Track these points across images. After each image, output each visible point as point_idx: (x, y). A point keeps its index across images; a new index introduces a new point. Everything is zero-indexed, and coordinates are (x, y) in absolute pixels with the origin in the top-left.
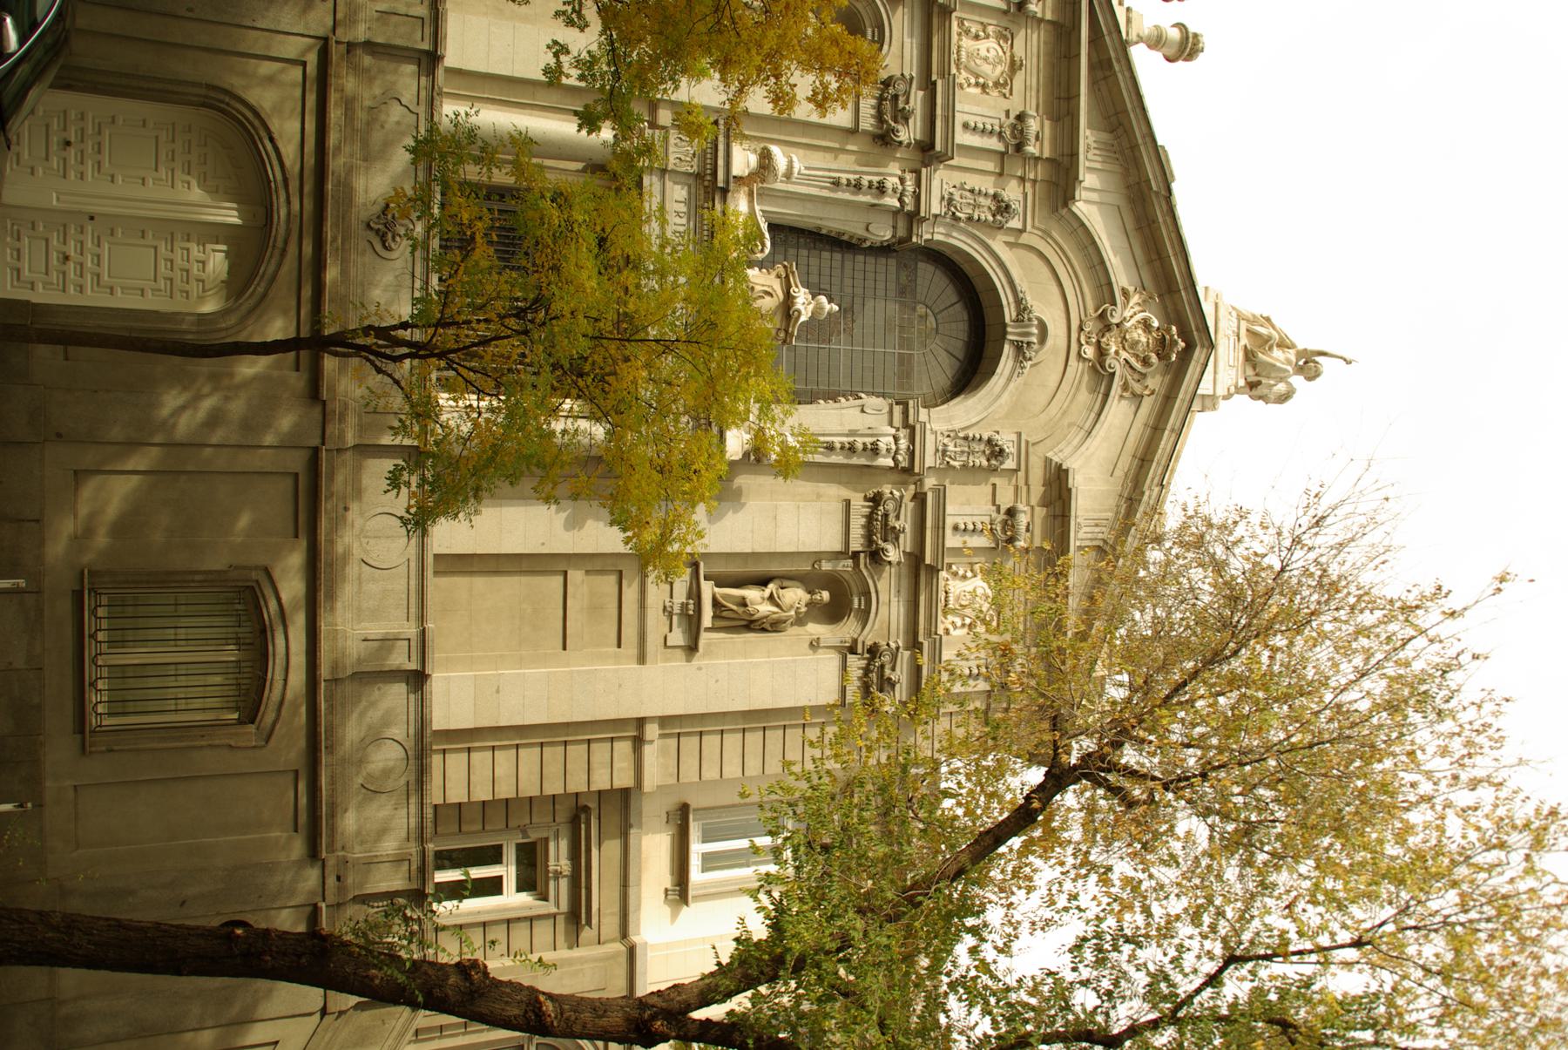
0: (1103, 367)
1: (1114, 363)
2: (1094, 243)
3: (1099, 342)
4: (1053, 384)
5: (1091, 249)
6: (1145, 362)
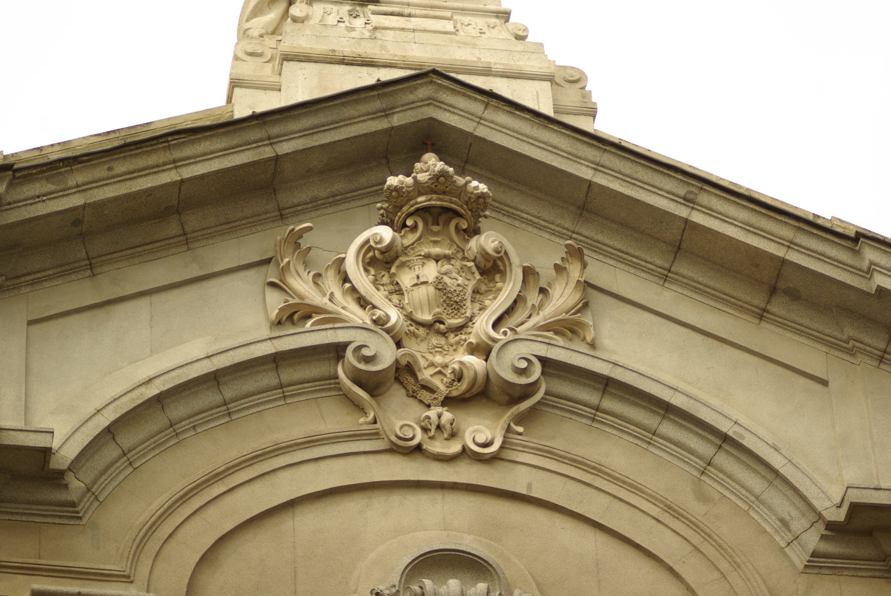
0: (527, 391)
1: (516, 354)
2: (160, 400)
3: (448, 402)
4: (590, 543)
5: (177, 411)
6: (491, 268)
